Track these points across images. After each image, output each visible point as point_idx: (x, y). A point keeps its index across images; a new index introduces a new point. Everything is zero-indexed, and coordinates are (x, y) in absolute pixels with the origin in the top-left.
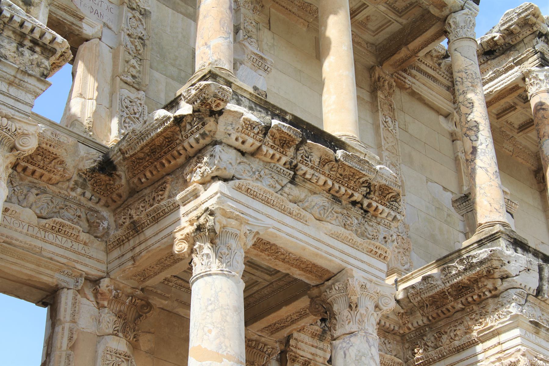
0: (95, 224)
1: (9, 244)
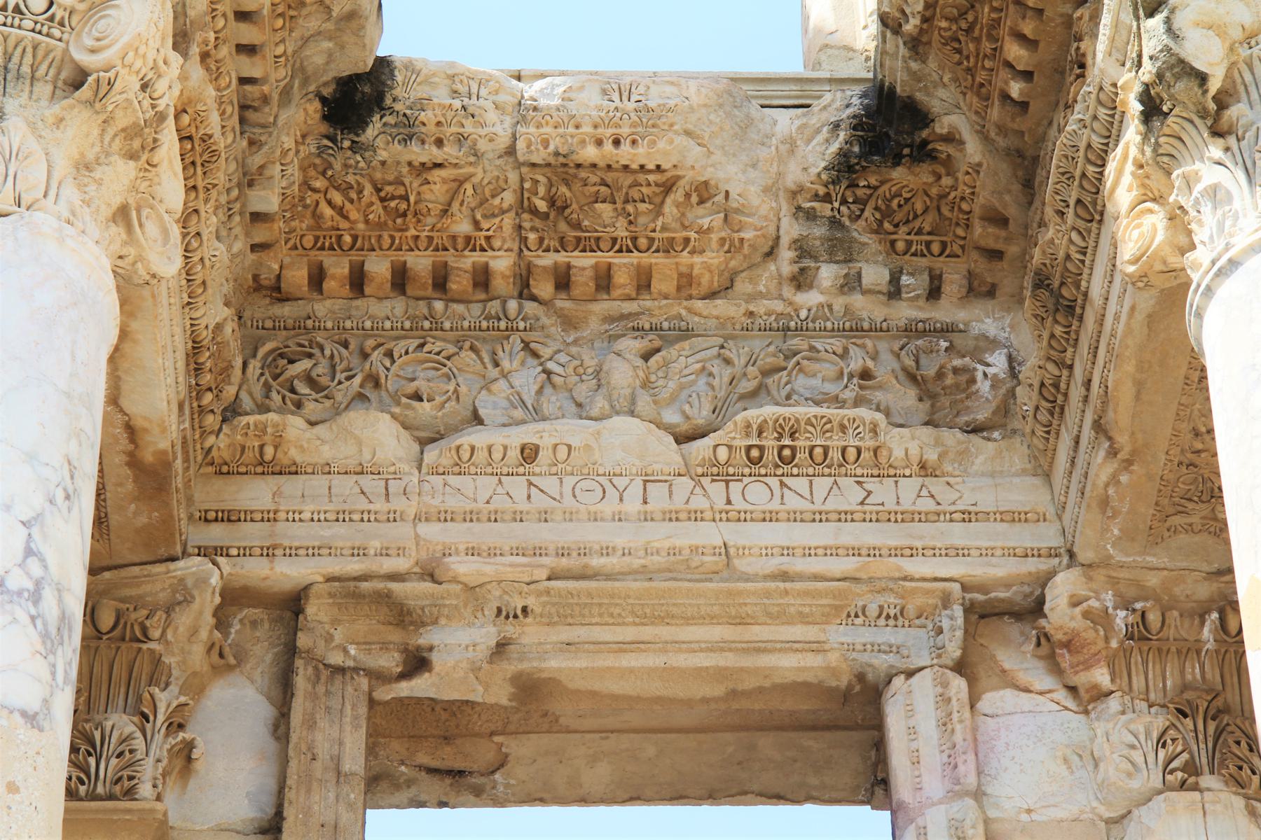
0: (949, 380)
1: (583, 575)
